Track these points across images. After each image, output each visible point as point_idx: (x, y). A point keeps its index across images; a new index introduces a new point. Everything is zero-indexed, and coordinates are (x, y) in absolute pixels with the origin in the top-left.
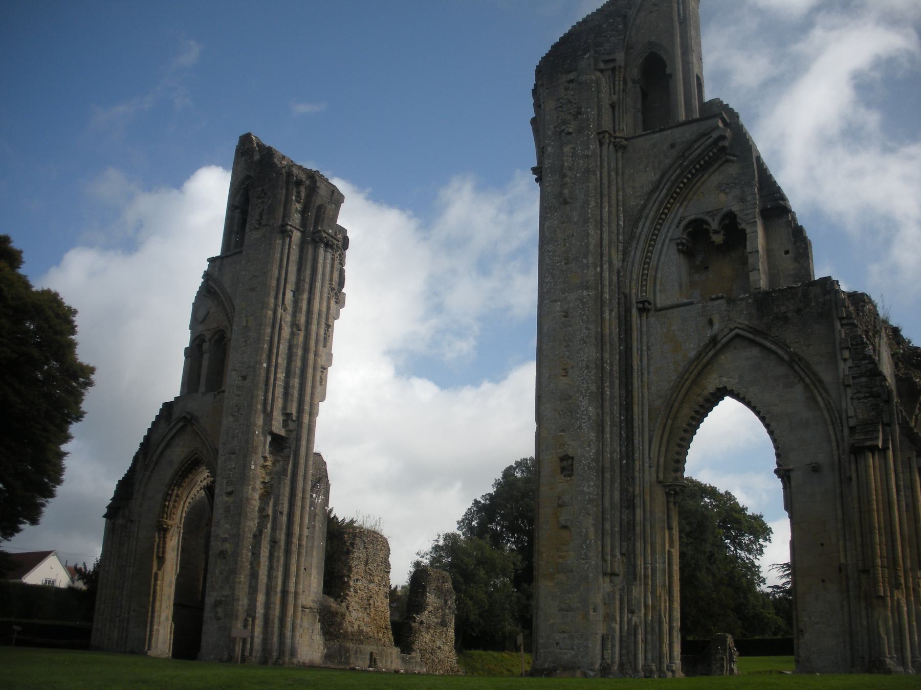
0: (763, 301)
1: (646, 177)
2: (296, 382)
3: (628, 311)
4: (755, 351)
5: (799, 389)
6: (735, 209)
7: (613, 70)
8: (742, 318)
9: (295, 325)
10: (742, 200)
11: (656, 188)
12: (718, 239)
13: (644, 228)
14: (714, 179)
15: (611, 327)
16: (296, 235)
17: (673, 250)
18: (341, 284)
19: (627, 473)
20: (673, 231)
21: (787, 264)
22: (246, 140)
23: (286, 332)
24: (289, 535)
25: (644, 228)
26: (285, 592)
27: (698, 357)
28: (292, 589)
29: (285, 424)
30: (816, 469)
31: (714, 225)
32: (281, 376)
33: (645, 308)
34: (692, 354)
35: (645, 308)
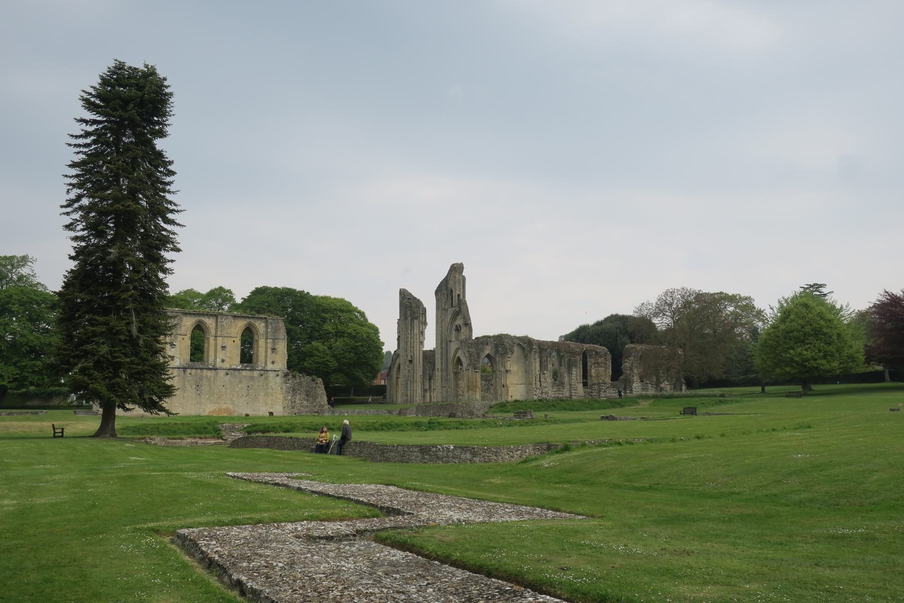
0: (462, 342)
1: (449, 316)
2: (412, 349)
9: (411, 337)
15: (444, 345)
16: (409, 318)
18: (425, 321)
19: (447, 370)
20: (454, 327)
22: (400, 289)
23: (409, 339)
24: (414, 379)
26: (414, 390)
28: (415, 389)
29: (411, 357)
32: (409, 348)
33: (450, 341)
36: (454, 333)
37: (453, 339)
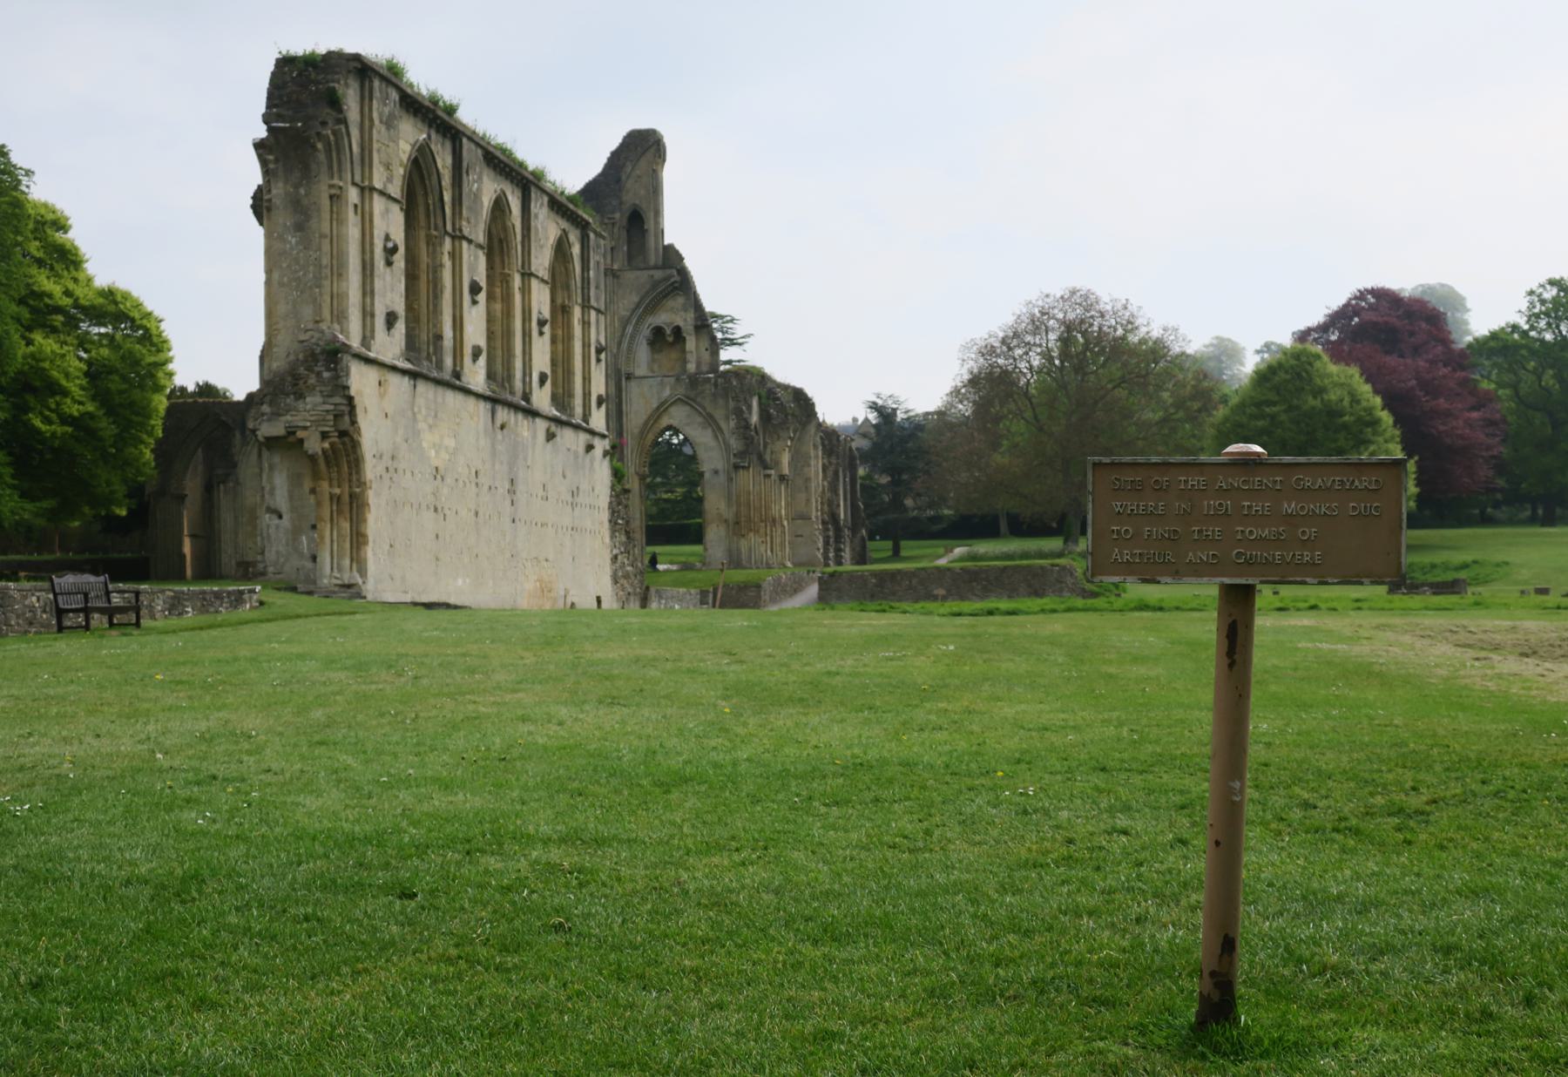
0: (694, 381)
3: (620, 380)
4: (687, 408)
5: (709, 431)
6: (681, 324)
7: (613, 224)
8: (681, 391)
10: (685, 320)
11: (638, 306)
12: (670, 339)
13: (630, 329)
14: (670, 303)
17: (645, 342)
20: (646, 332)
21: (706, 356)
25: (630, 329)
27: (658, 408)
30: (716, 472)
31: (668, 332)
33: (629, 377)
34: (655, 406)
35: (629, 377)
36: (643, 352)
37: (641, 370)
